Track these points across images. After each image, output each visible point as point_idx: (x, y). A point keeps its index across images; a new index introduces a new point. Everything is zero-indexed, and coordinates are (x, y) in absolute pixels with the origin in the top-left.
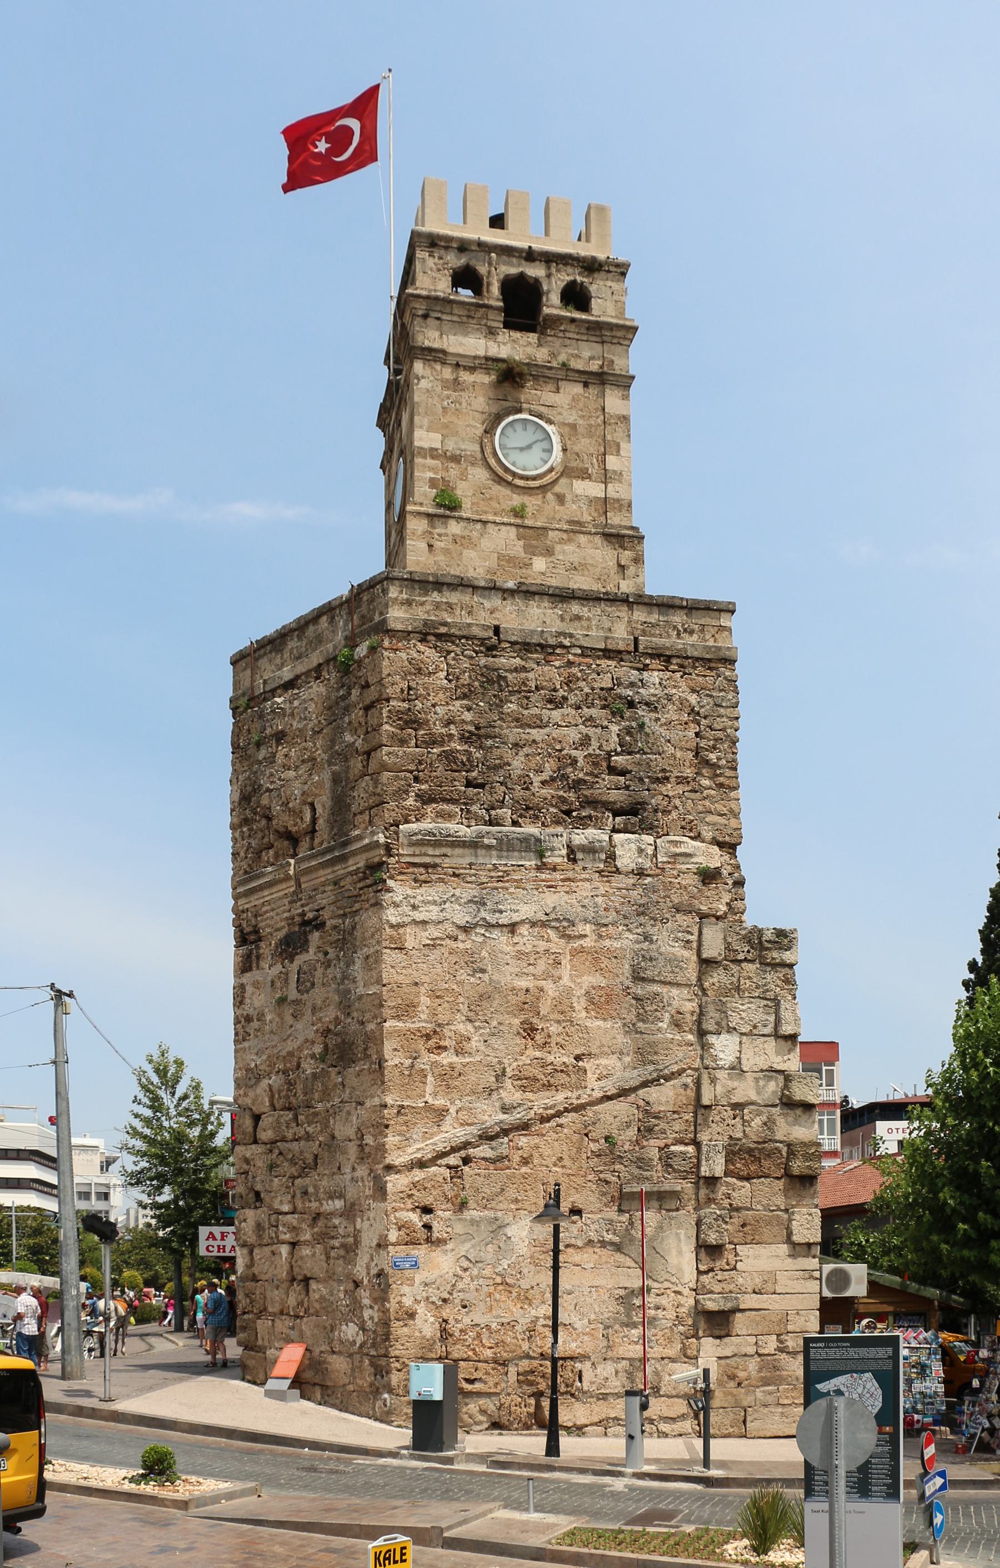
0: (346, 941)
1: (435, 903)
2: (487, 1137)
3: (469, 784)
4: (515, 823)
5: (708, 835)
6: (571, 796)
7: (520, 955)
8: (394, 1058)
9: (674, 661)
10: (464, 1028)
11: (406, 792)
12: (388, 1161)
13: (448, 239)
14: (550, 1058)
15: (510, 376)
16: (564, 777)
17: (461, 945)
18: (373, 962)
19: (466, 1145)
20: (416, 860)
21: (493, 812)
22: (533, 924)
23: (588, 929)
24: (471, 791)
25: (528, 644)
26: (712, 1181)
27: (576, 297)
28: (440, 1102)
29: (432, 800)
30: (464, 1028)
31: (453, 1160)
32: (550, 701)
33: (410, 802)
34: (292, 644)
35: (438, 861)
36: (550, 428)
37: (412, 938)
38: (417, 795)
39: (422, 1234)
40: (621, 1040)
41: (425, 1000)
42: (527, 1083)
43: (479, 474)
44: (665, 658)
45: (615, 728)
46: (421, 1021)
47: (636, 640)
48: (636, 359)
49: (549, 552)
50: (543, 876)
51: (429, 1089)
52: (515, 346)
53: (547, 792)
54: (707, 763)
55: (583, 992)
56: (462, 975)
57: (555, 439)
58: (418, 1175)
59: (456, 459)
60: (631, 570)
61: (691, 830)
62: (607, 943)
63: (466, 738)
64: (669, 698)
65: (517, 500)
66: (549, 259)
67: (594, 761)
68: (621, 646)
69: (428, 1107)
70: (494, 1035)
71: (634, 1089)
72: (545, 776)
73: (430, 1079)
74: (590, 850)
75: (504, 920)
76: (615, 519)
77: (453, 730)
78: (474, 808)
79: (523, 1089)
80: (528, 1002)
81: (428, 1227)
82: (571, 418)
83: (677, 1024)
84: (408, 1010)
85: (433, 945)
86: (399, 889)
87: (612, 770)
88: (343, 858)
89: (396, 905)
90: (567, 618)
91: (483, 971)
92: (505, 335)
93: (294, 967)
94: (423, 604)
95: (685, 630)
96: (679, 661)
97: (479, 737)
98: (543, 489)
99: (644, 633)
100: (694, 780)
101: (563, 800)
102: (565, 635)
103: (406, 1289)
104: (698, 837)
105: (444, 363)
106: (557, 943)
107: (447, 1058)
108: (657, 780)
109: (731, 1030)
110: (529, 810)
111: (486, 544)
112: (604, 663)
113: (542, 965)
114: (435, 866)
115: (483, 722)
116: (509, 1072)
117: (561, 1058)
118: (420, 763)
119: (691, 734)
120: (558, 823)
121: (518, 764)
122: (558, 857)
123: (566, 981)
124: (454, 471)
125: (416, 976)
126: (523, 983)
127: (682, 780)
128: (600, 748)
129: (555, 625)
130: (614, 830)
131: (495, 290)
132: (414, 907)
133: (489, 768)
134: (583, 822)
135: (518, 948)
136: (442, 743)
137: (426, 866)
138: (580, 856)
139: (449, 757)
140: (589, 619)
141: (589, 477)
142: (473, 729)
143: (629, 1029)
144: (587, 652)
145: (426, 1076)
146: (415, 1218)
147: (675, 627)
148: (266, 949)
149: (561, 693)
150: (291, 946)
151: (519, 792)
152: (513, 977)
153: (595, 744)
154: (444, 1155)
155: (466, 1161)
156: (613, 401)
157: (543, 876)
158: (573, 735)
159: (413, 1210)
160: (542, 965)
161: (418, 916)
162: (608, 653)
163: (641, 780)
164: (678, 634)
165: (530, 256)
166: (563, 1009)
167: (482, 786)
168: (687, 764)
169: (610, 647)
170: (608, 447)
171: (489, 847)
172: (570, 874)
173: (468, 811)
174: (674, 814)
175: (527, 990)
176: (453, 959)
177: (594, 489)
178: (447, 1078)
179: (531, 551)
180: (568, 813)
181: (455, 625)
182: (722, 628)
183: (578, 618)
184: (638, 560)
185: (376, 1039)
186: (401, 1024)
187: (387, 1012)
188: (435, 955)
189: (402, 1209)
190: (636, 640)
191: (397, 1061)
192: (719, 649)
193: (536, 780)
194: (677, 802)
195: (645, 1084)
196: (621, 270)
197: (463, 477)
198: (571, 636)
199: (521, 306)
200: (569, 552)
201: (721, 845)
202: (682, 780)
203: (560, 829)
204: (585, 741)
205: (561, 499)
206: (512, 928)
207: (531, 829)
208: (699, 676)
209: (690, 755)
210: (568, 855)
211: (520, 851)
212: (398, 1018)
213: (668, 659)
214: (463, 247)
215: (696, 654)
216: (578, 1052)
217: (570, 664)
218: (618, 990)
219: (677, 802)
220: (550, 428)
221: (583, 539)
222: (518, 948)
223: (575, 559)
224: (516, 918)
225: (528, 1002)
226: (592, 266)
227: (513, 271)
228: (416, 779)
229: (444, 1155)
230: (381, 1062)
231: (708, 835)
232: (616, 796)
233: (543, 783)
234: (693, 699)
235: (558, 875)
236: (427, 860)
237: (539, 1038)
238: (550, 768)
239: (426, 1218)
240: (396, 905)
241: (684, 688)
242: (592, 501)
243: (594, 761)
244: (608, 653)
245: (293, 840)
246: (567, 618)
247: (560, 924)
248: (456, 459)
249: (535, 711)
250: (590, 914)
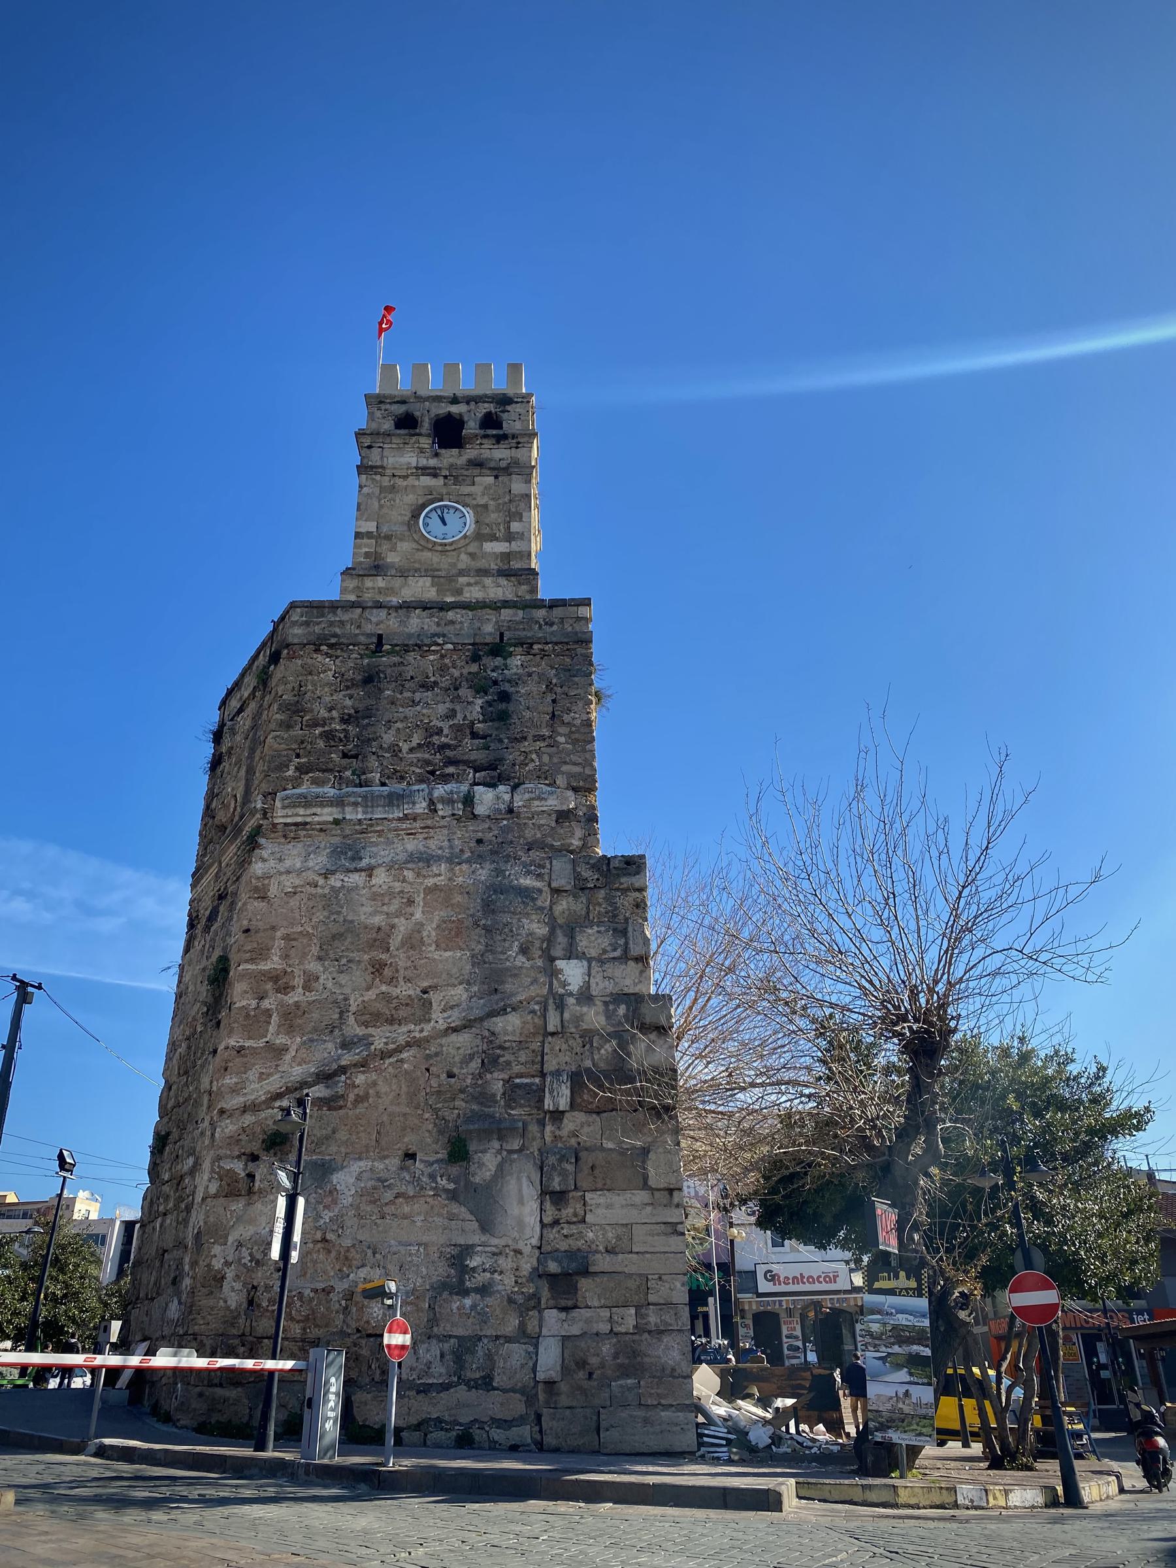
2: (325, 1077)
3: (345, 755)
4: (383, 784)
7: (374, 897)
9: (535, 647)
10: (313, 966)
11: (287, 767)
12: (222, 1104)
14: (395, 992)
17: (319, 890)
19: (304, 1084)
20: (289, 820)
21: (363, 777)
24: (345, 761)
25: (407, 645)
28: (281, 1040)
30: (313, 966)
32: (422, 686)
35: (308, 819)
38: (296, 768)
45: (479, 702)
46: (274, 963)
47: (502, 635)
50: (404, 826)
51: (272, 1029)
55: (434, 926)
61: (546, 779)
63: (343, 721)
67: (457, 729)
70: (342, 972)
72: (414, 743)
73: (275, 1018)
75: (364, 863)
77: (335, 713)
78: (348, 773)
79: (366, 1024)
80: (380, 939)
81: (251, 1176)
83: (524, 950)
87: (474, 735)
90: (443, 623)
94: (319, 623)
95: (546, 624)
96: (540, 646)
97: (357, 718)
99: (509, 628)
100: (550, 737)
101: (428, 762)
103: (217, 1249)
107: (292, 998)
114: (306, 823)
116: (353, 1009)
117: (404, 990)
118: (302, 742)
120: (421, 781)
121: (388, 738)
123: (418, 915)
126: (377, 920)
128: (465, 718)
129: (434, 629)
133: (363, 742)
134: (446, 779)
135: (374, 889)
137: (296, 824)
138: (440, 806)
139: (328, 736)
140: (461, 623)
142: (352, 711)
145: (271, 1016)
146: (238, 1167)
147: (537, 622)
149: (432, 679)
152: (368, 915)
153: (460, 716)
154: (279, 1096)
157: (404, 826)
158: (442, 709)
159: (239, 1157)
163: (501, 741)
164: (540, 626)
166: (413, 942)
167: (356, 757)
168: (544, 725)
169: (477, 641)
172: (429, 822)
173: (341, 777)
174: (531, 766)
175: (379, 929)
176: (311, 904)
180: (432, 773)
181: (344, 635)
182: (579, 619)
183: (452, 622)
186: (254, 967)
188: (294, 902)
189: (227, 1157)
190: (502, 635)
191: (244, 1003)
192: (576, 633)
193: (405, 747)
194: (534, 756)
198: (444, 636)
204: (452, 714)
210: (429, 805)
211: (384, 806)
215: (554, 639)
216: (425, 984)
218: (469, 922)
219: (534, 756)
222: (374, 889)
225: (380, 939)
229: (279, 1096)
232: (479, 756)
233: (411, 750)
236: (299, 819)
237: (387, 972)
239: (251, 1166)
240: (264, 860)
243: (457, 729)
246: (443, 623)
249: (407, 694)
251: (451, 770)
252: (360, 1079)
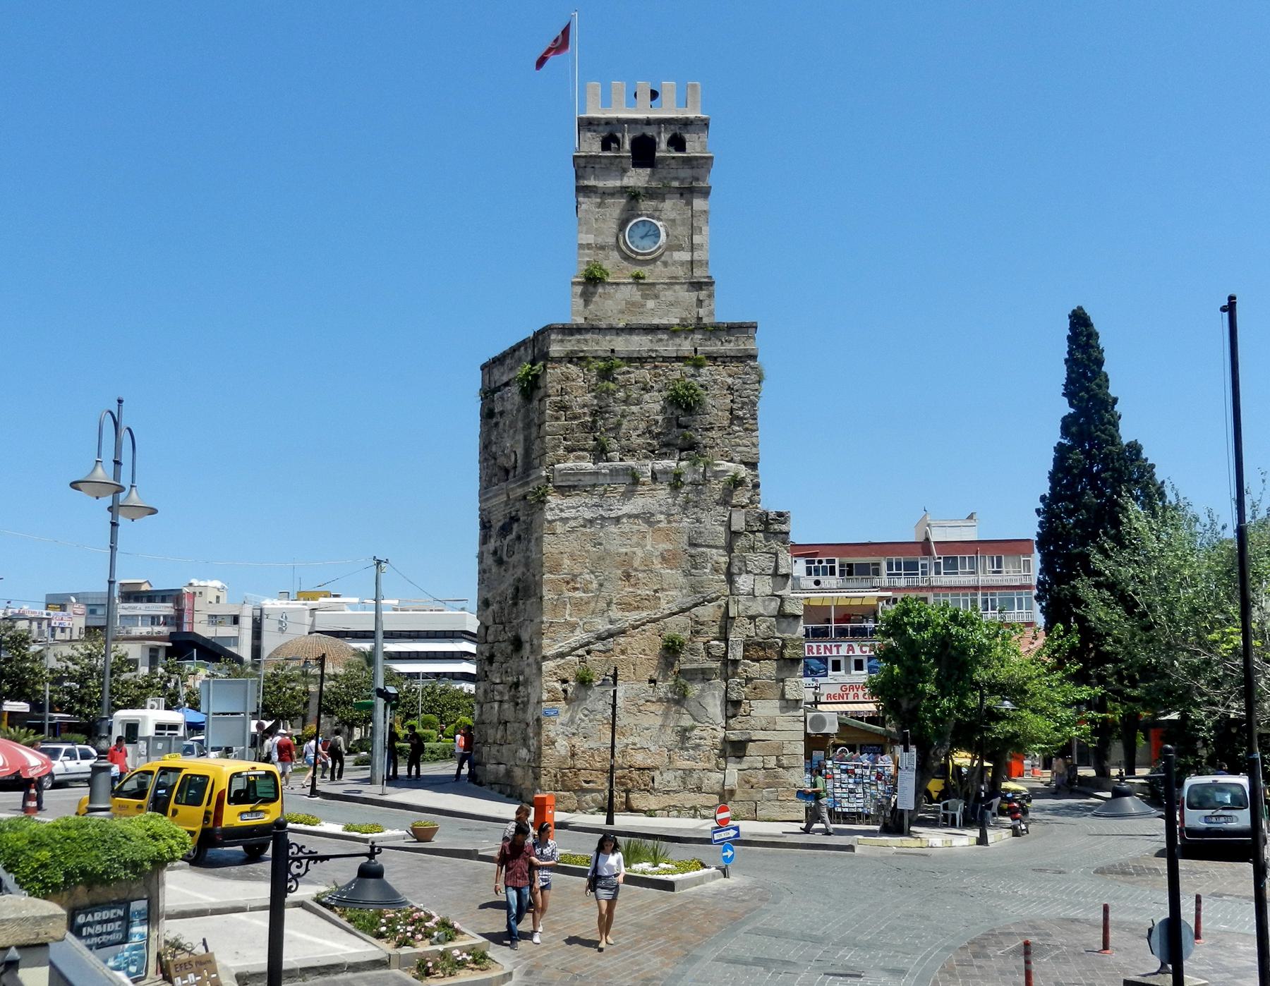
0: (529, 528)
1: (573, 508)
2: (600, 638)
4: (621, 460)
5: (737, 459)
6: (655, 442)
8: (548, 595)
13: (599, 119)
15: (633, 196)
16: (650, 432)
18: (539, 540)
19: (588, 644)
22: (630, 516)
23: (662, 517)
26: (735, 662)
27: (677, 143)
29: (573, 450)
31: (580, 652)
33: (561, 452)
34: (508, 361)
36: (659, 224)
37: (559, 528)
39: (562, 695)
40: (681, 580)
41: (567, 562)
42: (626, 606)
43: (616, 255)
44: (713, 358)
48: (713, 179)
49: (657, 297)
51: (568, 612)
52: (637, 178)
53: (641, 441)
54: (738, 417)
56: (589, 547)
57: (662, 230)
58: (560, 661)
59: (602, 248)
60: (706, 303)
62: (674, 524)
64: (715, 381)
65: (637, 270)
66: (659, 122)
68: (686, 354)
69: (567, 622)
71: (689, 609)
72: (639, 432)
74: (665, 472)
76: (699, 273)
77: (586, 410)
80: (627, 560)
81: (565, 691)
82: (673, 215)
84: (555, 569)
85: (573, 530)
86: (553, 500)
88: (527, 483)
89: (552, 509)
91: (600, 544)
92: (633, 172)
93: (506, 542)
98: (654, 260)
99: (701, 345)
102: (652, 351)
104: (731, 460)
105: (596, 192)
106: (644, 527)
108: (707, 430)
109: (748, 572)
110: (629, 451)
111: (619, 295)
112: (676, 365)
113: (635, 539)
115: (602, 404)
117: (644, 592)
119: (728, 401)
120: (646, 457)
122: (646, 478)
123: (648, 547)
124: (601, 254)
125: (562, 548)
126: (624, 550)
127: (720, 429)
130: (681, 460)
131: (627, 146)
132: (562, 511)
134: (662, 456)
136: (580, 418)
137: (569, 487)
141: (683, 249)
143: (687, 574)
144: (665, 359)
146: (558, 686)
148: (494, 532)
150: (505, 530)
151: (624, 442)
154: (577, 649)
155: (589, 652)
156: (698, 204)
160: (635, 539)
161: (564, 515)
162: (678, 359)
165: (648, 122)
170: (693, 230)
171: (605, 475)
177: (685, 256)
178: (578, 605)
179: (645, 297)
180: (653, 452)
184: (710, 296)
185: (539, 585)
187: (545, 569)
193: (634, 434)
195: (695, 605)
196: (704, 124)
197: (607, 257)
199: (644, 153)
200: (668, 295)
201: (746, 464)
202: (720, 429)
203: (647, 461)
205: (665, 264)
206: (618, 520)
207: (630, 462)
208: (733, 368)
209: (727, 413)
212: (551, 572)
213: (715, 359)
214: (608, 122)
217: (656, 367)
220: (659, 224)
221: (677, 287)
223: (672, 299)
224: (620, 513)
226: (686, 123)
227: (638, 134)
228: (565, 439)
230: (541, 598)
231: (737, 459)
234: (730, 380)
235: (645, 488)
237: (633, 581)
238: (642, 425)
240: (552, 509)
241: (724, 374)
242: (682, 264)
244: (678, 359)
245: (507, 471)
247: (647, 517)
248: (602, 248)
250: (664, 509)
251: (664, 450)
252: (621, 640)
